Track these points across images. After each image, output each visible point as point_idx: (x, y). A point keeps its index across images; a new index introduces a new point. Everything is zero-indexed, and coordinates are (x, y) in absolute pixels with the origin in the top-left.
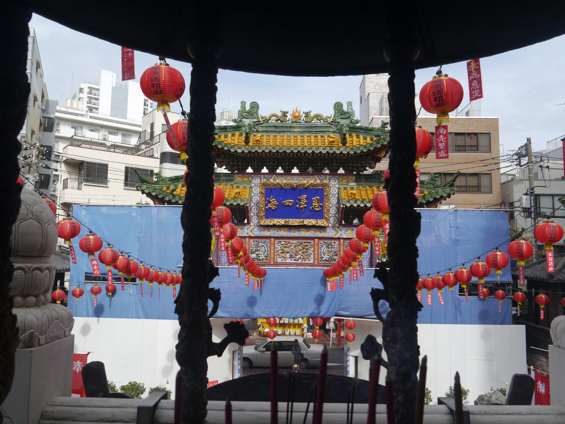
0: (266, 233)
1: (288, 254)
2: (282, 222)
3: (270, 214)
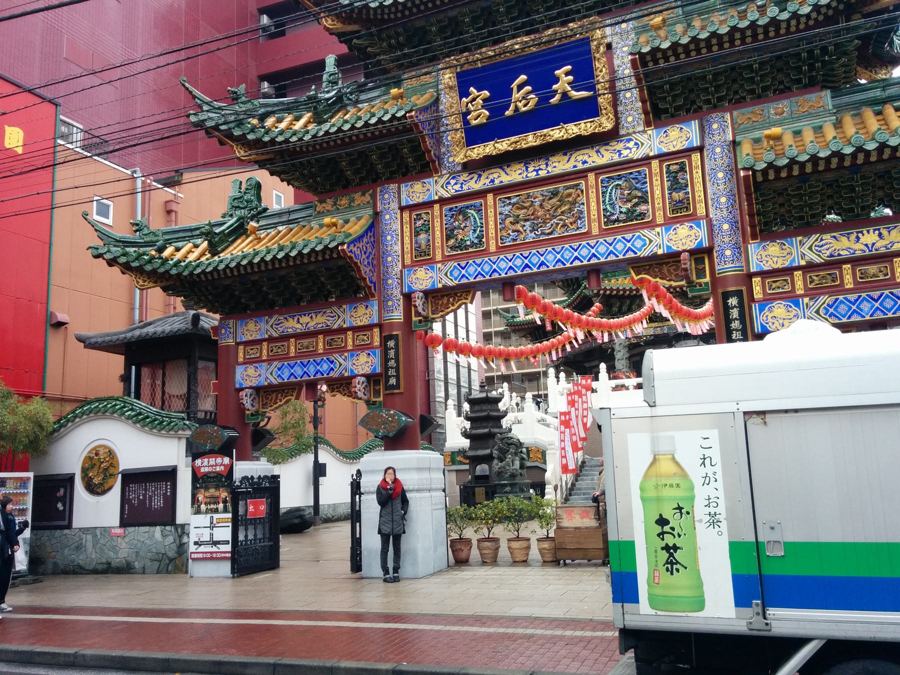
0: (475, 184)
1: (528, 223)
2: (503, 145)
3: (474, 136)
